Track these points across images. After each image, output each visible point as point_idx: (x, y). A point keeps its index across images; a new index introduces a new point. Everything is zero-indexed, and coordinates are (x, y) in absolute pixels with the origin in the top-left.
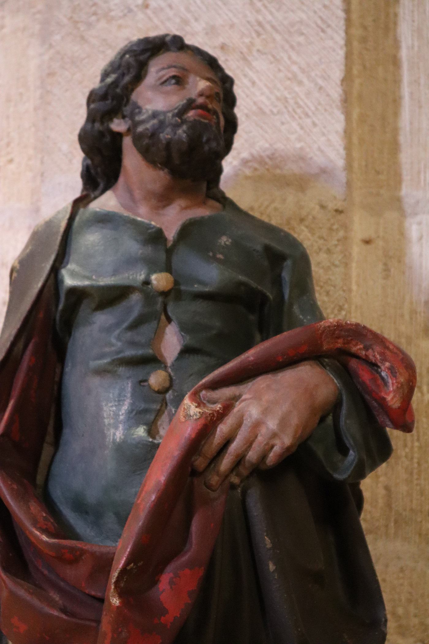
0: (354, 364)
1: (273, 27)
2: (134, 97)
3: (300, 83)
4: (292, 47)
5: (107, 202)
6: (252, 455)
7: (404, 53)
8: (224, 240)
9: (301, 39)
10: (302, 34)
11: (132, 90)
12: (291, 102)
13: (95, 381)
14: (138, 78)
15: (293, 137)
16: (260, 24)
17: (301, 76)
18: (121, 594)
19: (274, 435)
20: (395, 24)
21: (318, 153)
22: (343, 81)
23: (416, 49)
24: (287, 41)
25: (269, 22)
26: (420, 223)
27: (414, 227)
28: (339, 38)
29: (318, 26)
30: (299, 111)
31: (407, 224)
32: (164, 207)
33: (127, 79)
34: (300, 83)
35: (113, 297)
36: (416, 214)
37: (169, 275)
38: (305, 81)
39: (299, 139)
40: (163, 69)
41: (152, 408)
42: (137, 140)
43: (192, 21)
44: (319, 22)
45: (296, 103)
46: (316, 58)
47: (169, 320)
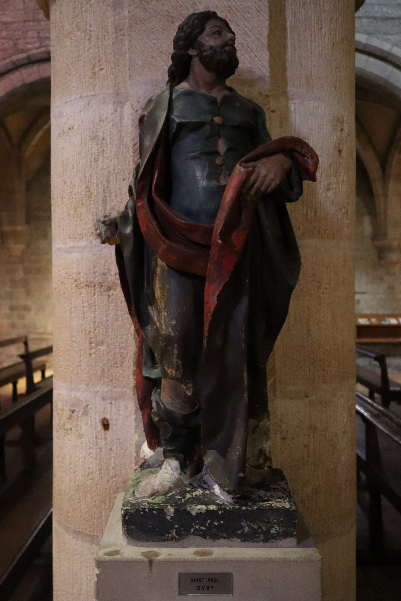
0: (296, 155)
1: (236, 9)
2: (199, 39)
3: (249, 36)
4: (245, 19)
5: (184, 86)
6: (263, 188)
7: (288, 24)
8: (237, 104)
9: (249, 15)
10: (250, 13)
11: (198, 37)
12: (245, 45)
13: (192, 163)
14: (202, 31)
15: (246, 62)
16: (230, 7)
17: (250, 34)
18: (221, 239)
19: (272, 180)
20: (285, 10)
21: (258, 69)
22: (268, 36)
23: (293, 22)
24: (243, 16)
25: (234, 6)
26: (294, 104)
27: (292, 105)
28: (266, 15)
29: (257, 10)
30: (249, 49)
31: (289, 104)
32: (213, 89)
33: (197, 31)
34: (249, 36)
35: (196, 127)
36: (293, 99)
37: (219, 117)
38: (251, 35)
39: (249, 63)
40: (212, 27)
41: (214, 173)
42: (202, 60)
43: (198, 3)
44: (257, 7)
45: (248, 46)
46: (256, 25)
47: (220, 137)
